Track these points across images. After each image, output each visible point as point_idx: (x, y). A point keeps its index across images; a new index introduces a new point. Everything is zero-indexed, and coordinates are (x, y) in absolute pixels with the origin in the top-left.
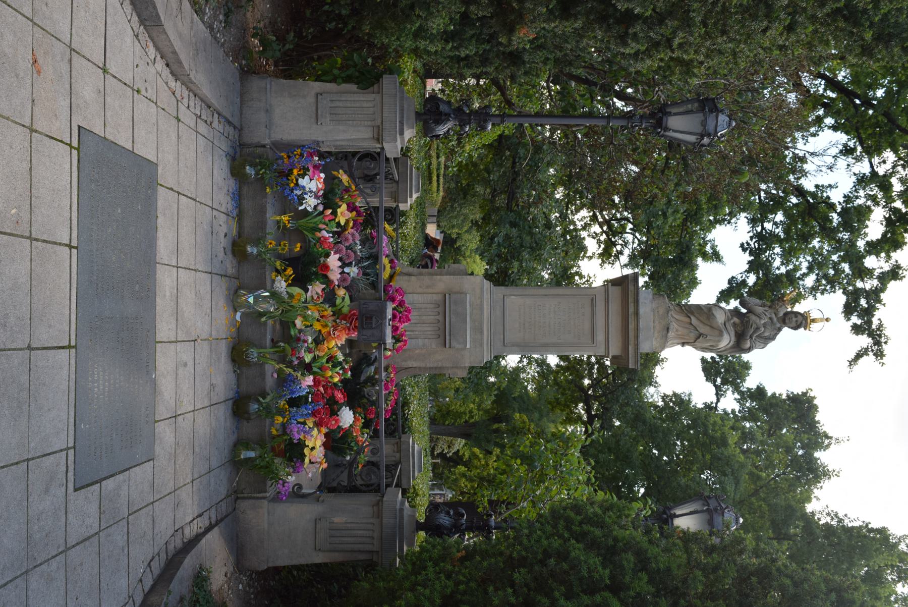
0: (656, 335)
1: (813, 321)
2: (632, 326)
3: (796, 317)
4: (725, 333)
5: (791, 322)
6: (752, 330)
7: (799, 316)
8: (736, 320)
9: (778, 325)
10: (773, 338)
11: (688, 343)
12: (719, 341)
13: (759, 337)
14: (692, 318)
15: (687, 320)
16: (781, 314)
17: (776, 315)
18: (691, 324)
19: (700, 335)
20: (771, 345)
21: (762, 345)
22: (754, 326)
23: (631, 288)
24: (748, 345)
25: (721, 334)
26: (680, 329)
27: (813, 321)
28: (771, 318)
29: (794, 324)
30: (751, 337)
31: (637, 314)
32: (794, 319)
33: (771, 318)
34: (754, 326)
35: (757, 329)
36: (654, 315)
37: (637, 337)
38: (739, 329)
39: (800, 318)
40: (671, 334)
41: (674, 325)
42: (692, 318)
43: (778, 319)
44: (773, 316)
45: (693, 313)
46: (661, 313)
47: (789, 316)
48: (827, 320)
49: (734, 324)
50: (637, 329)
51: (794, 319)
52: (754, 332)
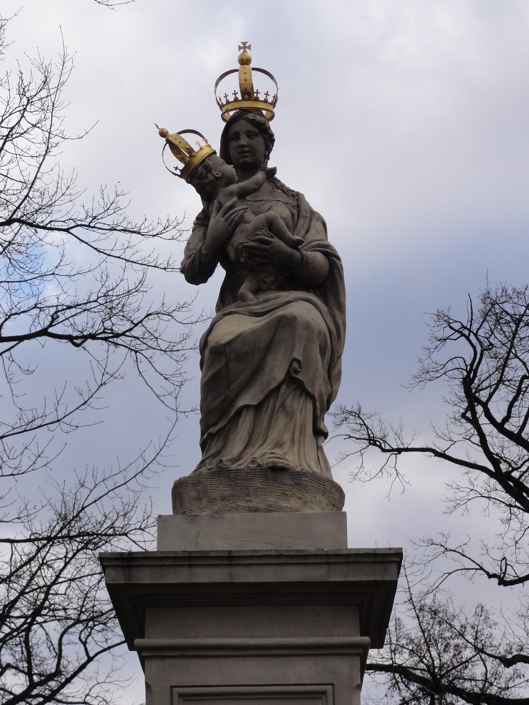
0: (293, 503)
1: (248, 92)
3: (237, 136)
4: (280, 312)
5: (253, 151)
6: (276, 241)
7: (237, 127)
8: (244, 289)
9: (260, 176)
10: (296, 198)
11: (317, 419)
12: (307, 326)
13: (294, 228)
14: (242, 402)
16: (230, 169)
17: (230, 181)
18: (258, 408)
19: (293, 381)
20: (315, 201)
21: (316, 225)
22: (264, 234)
23: (145, 577)
24: (319, 257)
25: (287, 323)
26: (274, 435)
27: (248, 92)
28: (243, 195)
29: (259, 142)
30: (295, 245)
31: (230, 559)
32: (244, 140)
33: (243, 195)
34: (264, 234)
35: (271, 225)
36: (237, 509)
37: (300, 558)
39: (242, 126)
40: (291, 459)
41: (263, 453)
42: (242, 402)
43: (242, 179)
44: (234, 187)
46: (227, 492)
47: (233, 153)
48: (244, 61)
49: (257, 291)
50: (281, 558)
51: (244, 140)
52: (281, 236)
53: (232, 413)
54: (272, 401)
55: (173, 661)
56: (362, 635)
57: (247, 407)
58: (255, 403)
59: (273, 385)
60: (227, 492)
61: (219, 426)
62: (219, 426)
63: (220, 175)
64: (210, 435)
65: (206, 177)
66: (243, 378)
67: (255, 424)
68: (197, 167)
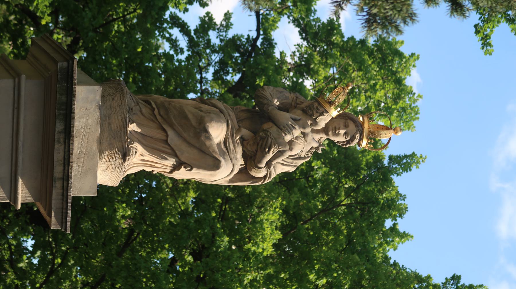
2: (58, 156)
14: (170, 132)
15: (160, 135)
18: (166, 142)
38: (251, 148)
42: (170, 132)
45: (172, 126)
49: (242, 139)
53: (165, 127)
54: (169, 151)
55: (12, 96)
56: (22, 204)
57: (167, 136)
58: (168, 141)
59: (178, 153)
60: (113, 126)
61: (158, 117)
62: (158, 117)
63: (317, 121)
64: (154, 109)
65: (317, 112)
66: (185, 135)
67: (157, 140)
68: (322, 107)
